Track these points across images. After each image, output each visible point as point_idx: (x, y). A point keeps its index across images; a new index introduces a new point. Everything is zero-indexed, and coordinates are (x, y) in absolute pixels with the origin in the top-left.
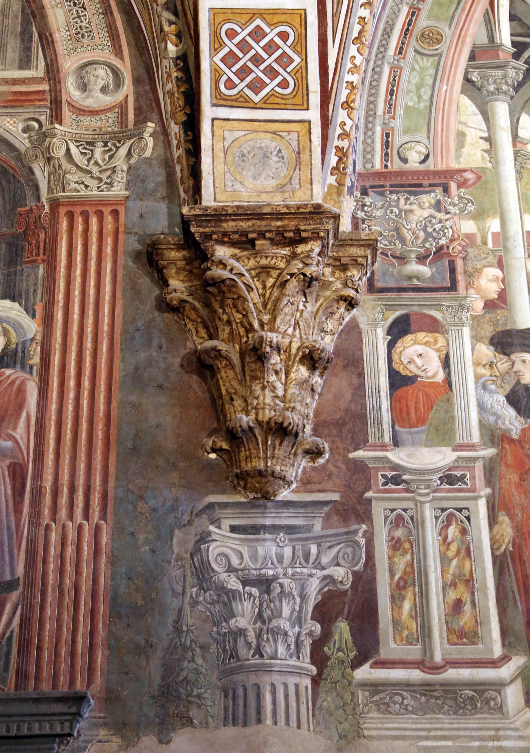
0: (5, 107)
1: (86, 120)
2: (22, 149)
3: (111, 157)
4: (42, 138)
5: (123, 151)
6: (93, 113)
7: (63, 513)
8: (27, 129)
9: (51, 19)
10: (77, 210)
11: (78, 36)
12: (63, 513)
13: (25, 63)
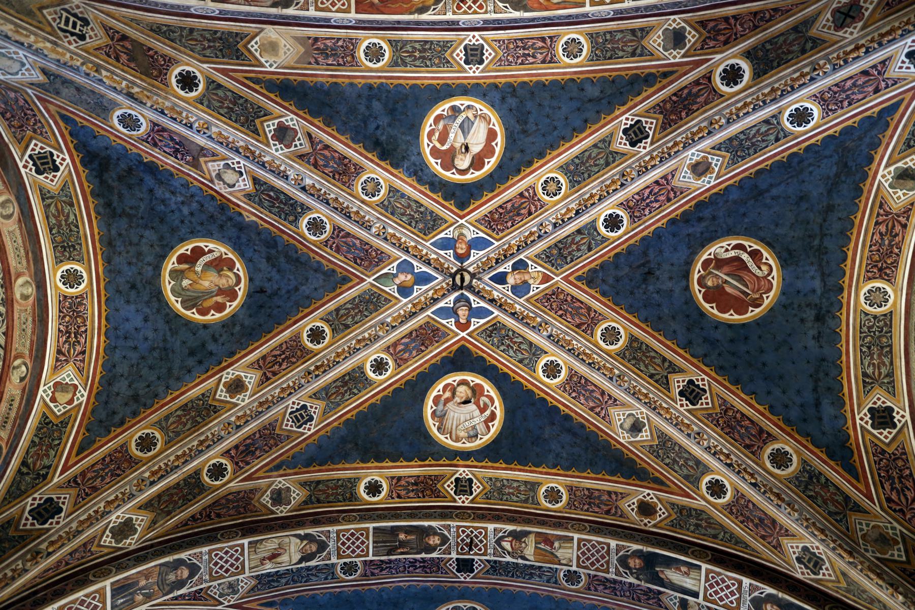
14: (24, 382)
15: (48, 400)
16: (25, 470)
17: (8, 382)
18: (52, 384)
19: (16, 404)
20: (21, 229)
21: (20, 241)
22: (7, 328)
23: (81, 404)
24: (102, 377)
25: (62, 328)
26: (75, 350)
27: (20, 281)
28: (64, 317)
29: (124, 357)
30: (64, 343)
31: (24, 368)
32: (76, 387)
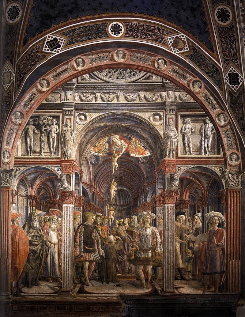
0: (215, 164)
1: (232, 168)
2: (220, 175)
3: (238, 178)
4: (223, 172)
5: (240, 177)
6: (234, 166)
7: (232, 258)
8: (220, 170)
9: (224, 141)
10: (232, 191)
11: (229, 146)
12: (232, 258)
13: (219, 153)
14: (167, 62)
15: (180, 52)
16: (210, 75)
17: (164, 72)
18: (172, 48)
19: (177, 69)
20: (89, 55)
21: (96, 56)
22: (137, 69)
23: (187, 38)
24: (175, 23)
25: (143, 37)
26: (157, 33)
27: (116, 58)
28: (137, 35)
29: (166, 8)
30: (152, 37)
31: (160, 61)
32: (177, 37)
